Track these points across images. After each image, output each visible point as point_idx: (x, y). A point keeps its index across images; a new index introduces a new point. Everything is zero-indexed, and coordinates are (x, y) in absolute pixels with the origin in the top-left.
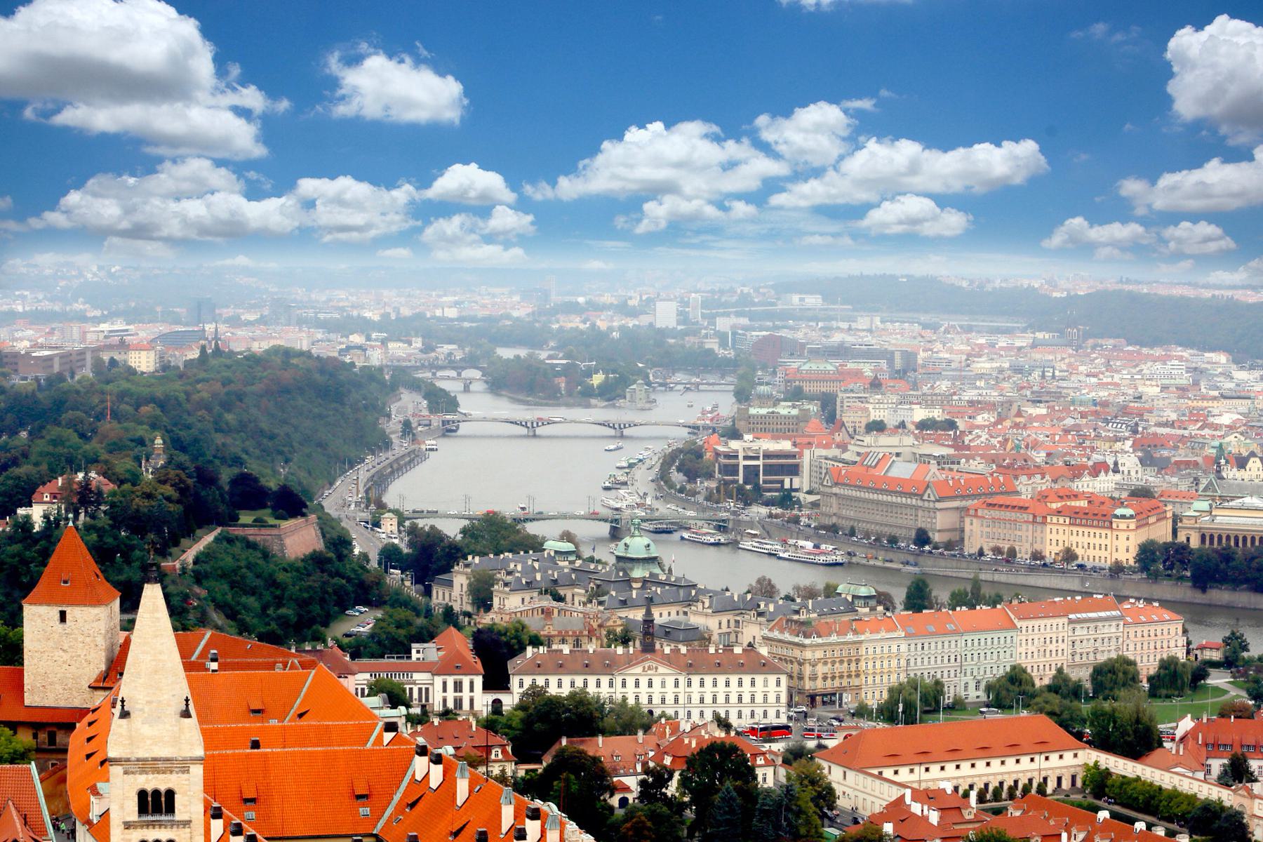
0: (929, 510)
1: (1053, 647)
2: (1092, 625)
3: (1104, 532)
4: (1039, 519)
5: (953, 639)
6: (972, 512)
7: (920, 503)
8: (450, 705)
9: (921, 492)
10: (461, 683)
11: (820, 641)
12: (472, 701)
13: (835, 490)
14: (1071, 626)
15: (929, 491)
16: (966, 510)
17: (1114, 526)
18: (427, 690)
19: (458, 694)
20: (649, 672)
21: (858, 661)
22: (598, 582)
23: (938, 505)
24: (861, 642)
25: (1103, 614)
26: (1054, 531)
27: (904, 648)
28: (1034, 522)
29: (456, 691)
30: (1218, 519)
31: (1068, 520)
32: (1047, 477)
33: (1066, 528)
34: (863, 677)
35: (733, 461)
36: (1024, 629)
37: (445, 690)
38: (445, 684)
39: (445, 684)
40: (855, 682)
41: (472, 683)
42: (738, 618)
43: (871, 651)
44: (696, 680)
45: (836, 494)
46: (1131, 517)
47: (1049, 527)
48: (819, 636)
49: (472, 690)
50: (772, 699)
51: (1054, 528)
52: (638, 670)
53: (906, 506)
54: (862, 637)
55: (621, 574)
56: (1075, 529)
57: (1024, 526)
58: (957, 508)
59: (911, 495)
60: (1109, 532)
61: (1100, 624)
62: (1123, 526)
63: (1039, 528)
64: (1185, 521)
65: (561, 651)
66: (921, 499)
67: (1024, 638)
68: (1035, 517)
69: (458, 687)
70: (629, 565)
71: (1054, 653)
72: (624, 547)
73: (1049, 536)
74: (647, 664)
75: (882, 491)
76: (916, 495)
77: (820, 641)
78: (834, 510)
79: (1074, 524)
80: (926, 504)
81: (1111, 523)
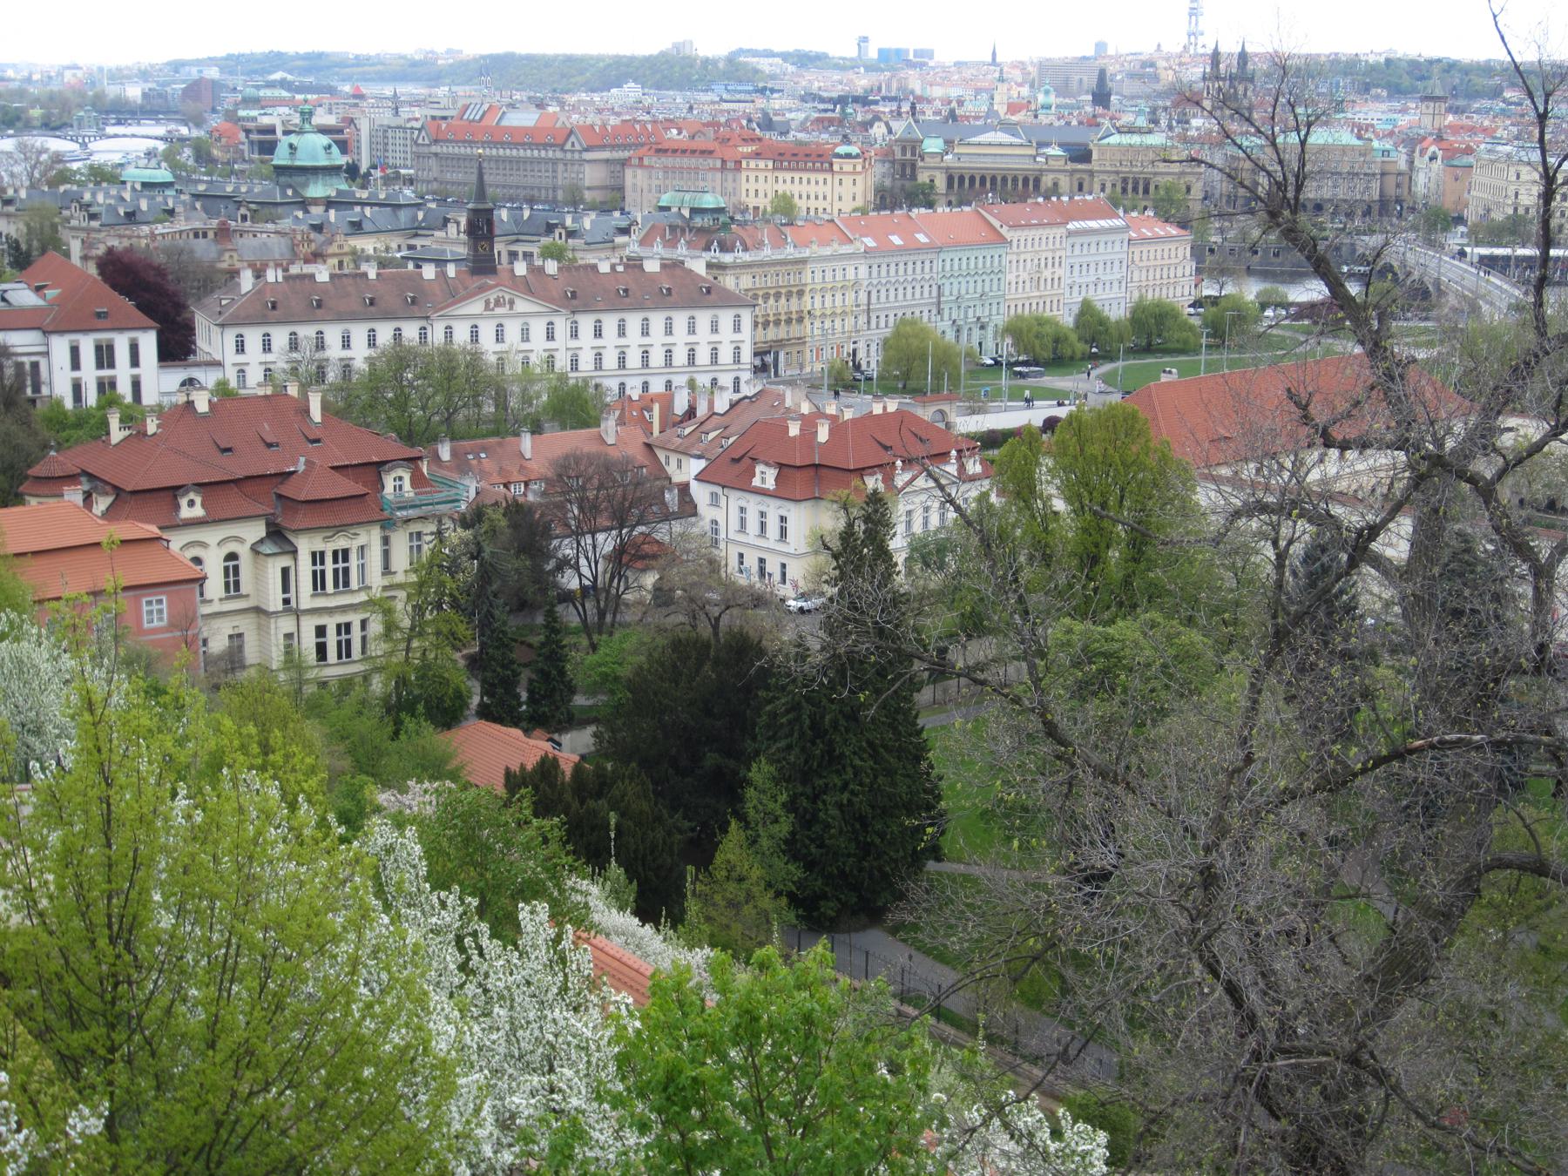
0: (573, 161)
1: (1047, 274)
2: (1094, 239)
3: (820, 177)
4: (730, 165)
5: (927, 258)
6: (635, 161)
7: (559, 155)
8: (91, 397)
9: (560, 141)
10: (111, 348)
11: (747, 257)
12: (136, 385)
13: (434, 149)
14: (1071, 240)
15: (572, 139)
16: (624, 163)
17: (836, 168)
18: (35, 366)
19: (106, 373)
20: (499, 311)
21: (801, 293)
22: (253, 206)
23: (588, 156)
24: (804, 261)
25: (1093, 224)
26: (752, 179)
27: (863, 271)
28: (723, 168)
29: (100, 365)
31: (770, 164)
32: (685, 132)
33: (769, 175)
34: (807, 322)
35: (269, 137)
36: (1015, 244)
37: (76, 364)
38: (75, 352)
39: (75, 352)
40: (795, 331)
41: (134, 349)
42: (514, 248)
43: (818, 276)
44: (586, 323)
45: (436, 155)
46: (857, 156)
47: (744, 175)
48: (746, 249)
49: (135, 362)
50: (726, 356)
51: (752, 176)
52: (476, 307)
53: (539, 161)
54: (806, 253)
55: (290, 192)
56: (781, 175)
57: (710, 175)
58: (607, 161)
59: (546, 146)
60: (829, 177)
61: (1103, 238)
62: (848, 168)
63: (730, 176)
64: (927, 159)
65: (312, 276)
66: (562, 149)
67: (1014, 258)
68: (724, 162)
69: (105, 356)
70: (299, 179)
72: (288, 150)
73: (744, 186)
74: (492, 295)
75: (503, 145)
76: (552, 145)
77: (747, 257)
78: (435, 173)
79: (781, 169)
80: (569, 156)
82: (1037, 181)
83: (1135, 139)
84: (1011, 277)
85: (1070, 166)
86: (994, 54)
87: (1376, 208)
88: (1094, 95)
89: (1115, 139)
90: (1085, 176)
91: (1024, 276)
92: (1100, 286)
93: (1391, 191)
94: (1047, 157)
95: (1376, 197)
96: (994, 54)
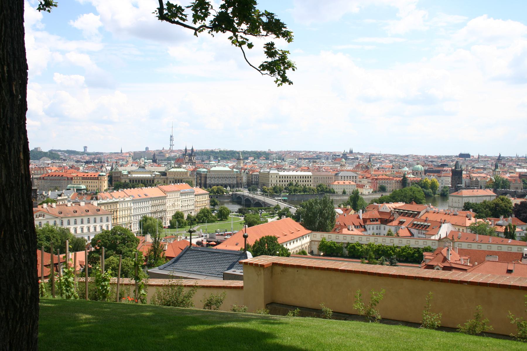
17: (99, 179)
21: (117, 211)
24: (117, 202)
30: (133, 175)
51: (76, 181)
60: (97, 181)
64: (124, 176)
71: (168, 207)
81: (98, 178)
82: (153, 181)
83: (178, 170)
84: (167, 205)
85: (162, 177)
86: (121, 150)
87: (236, 185)
88: (152, 160)
89: (173, 170)
90: (165, 179)
91: (171, 204)
92: (189, 206)
93: (239, 181)
94: (155, 175)
95: (236, 183)
96: (121, 150)
